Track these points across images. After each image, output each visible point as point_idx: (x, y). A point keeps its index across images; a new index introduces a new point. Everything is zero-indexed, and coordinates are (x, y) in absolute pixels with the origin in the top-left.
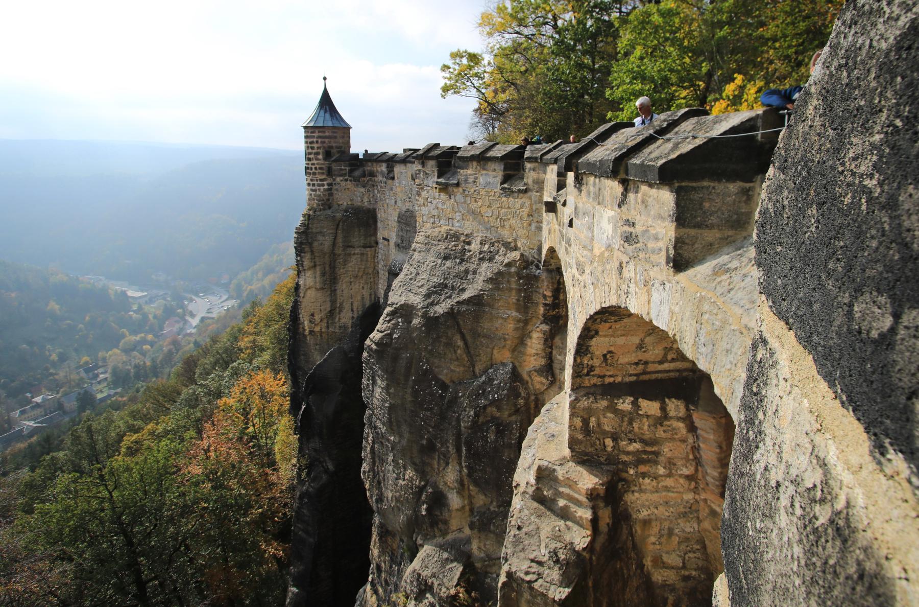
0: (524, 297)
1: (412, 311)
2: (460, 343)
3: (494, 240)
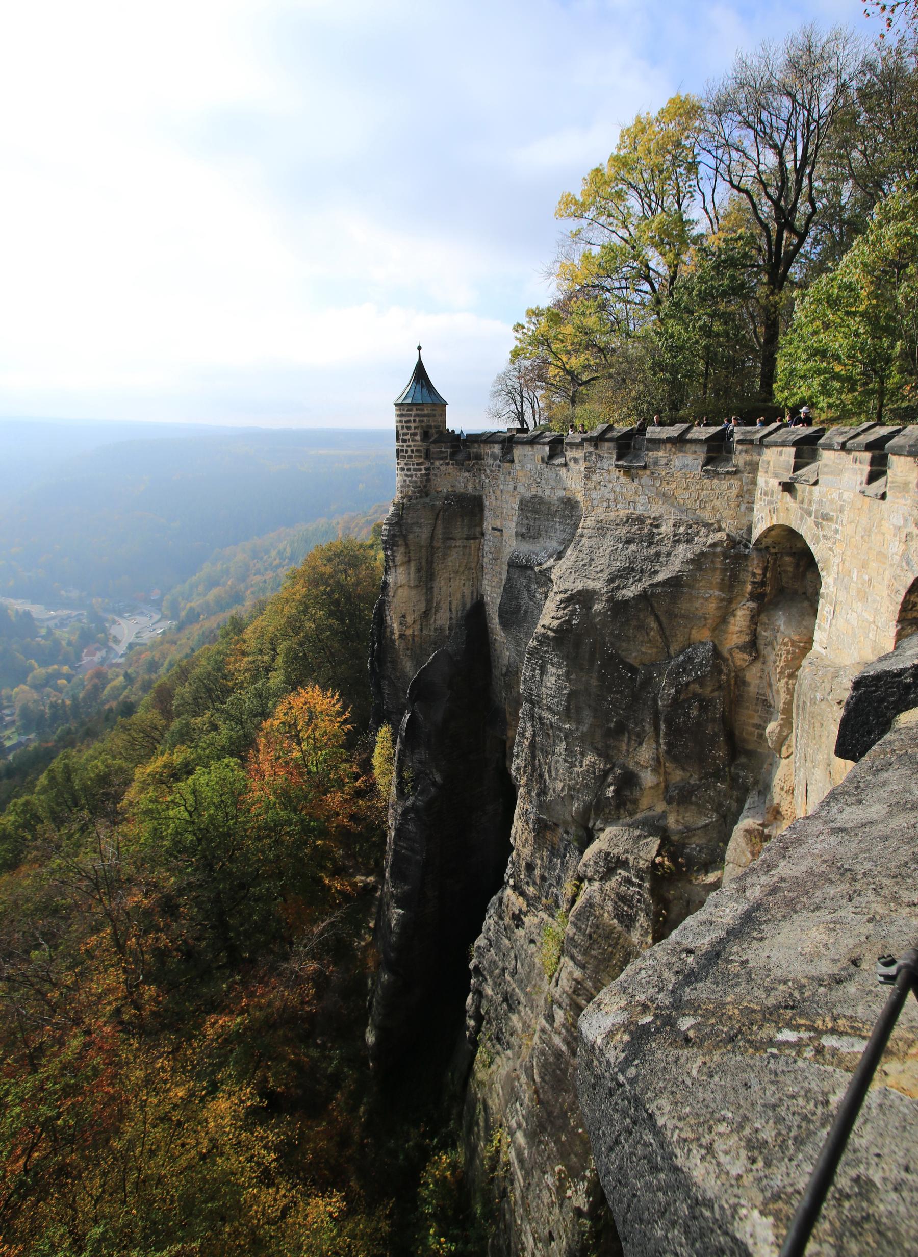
0: (731, 576)
1: (592, 596)
2: (654, 625)
3: (691, 522)
